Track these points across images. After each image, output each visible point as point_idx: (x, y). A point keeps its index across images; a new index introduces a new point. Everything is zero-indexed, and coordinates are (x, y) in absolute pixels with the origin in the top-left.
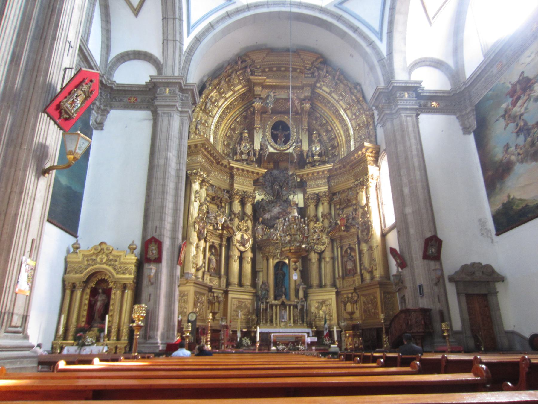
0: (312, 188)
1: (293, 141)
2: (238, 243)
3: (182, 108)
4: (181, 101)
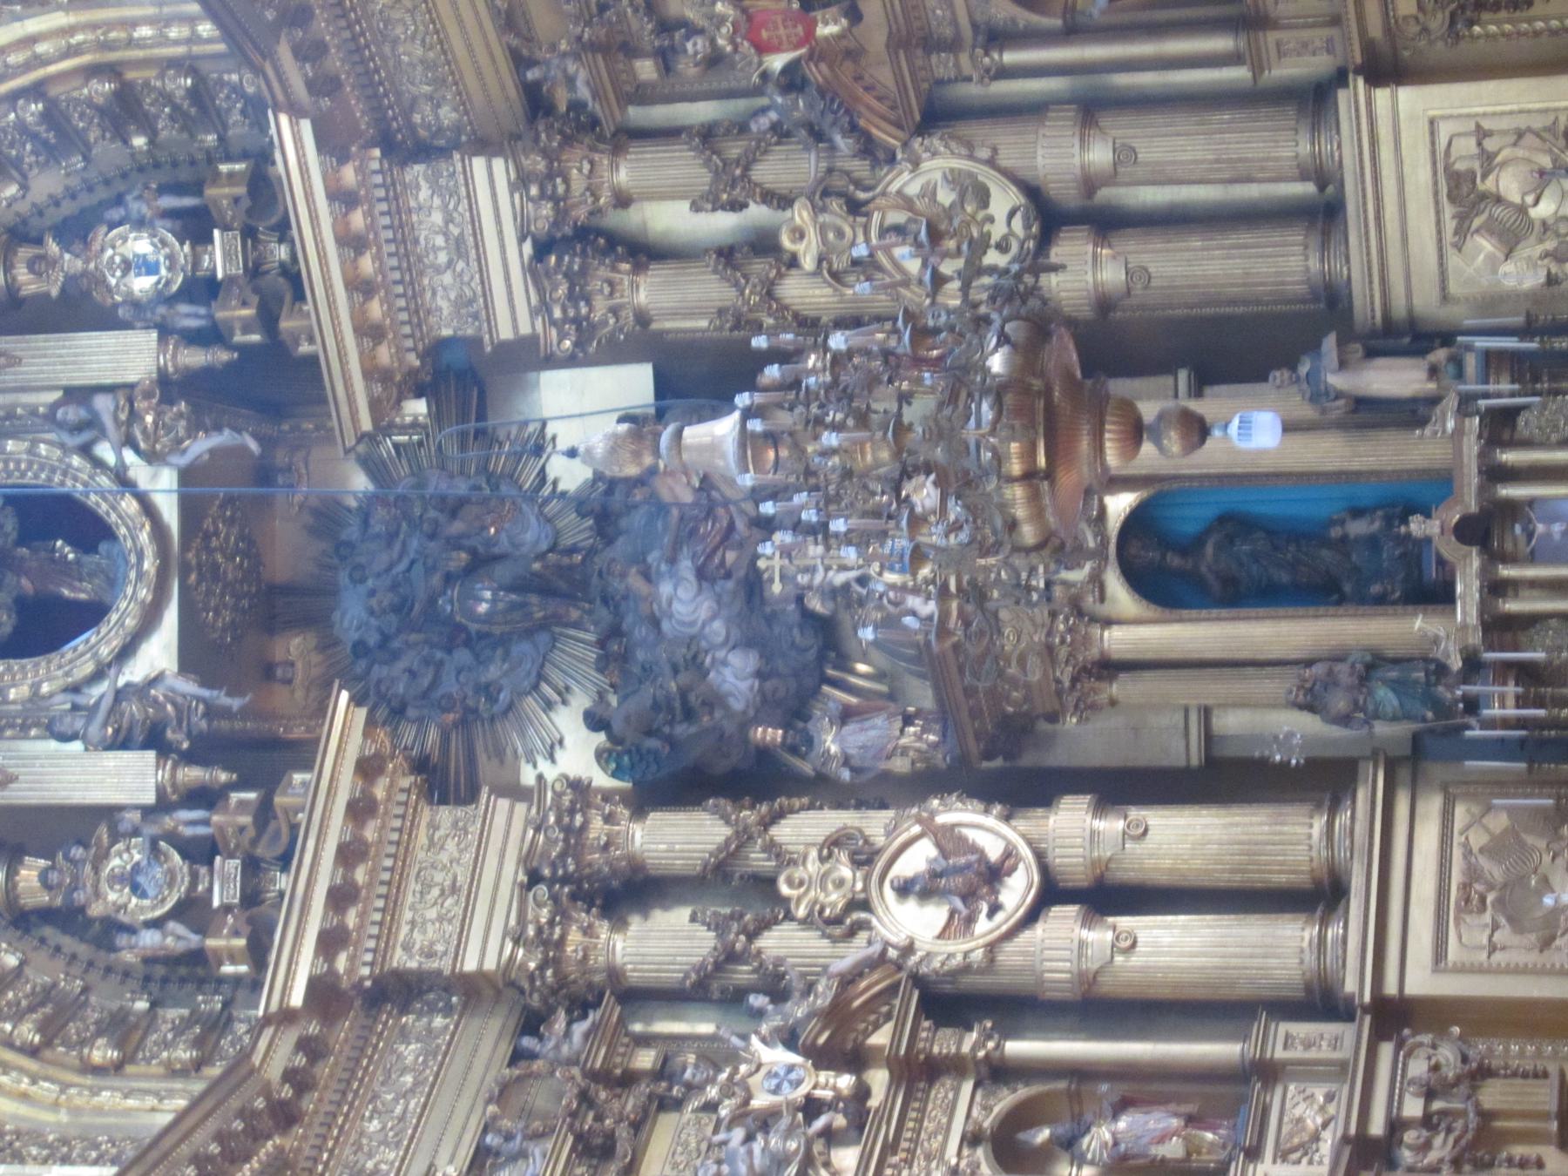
0: (487, 292)
1: (76, 461)
2: (970, 920)
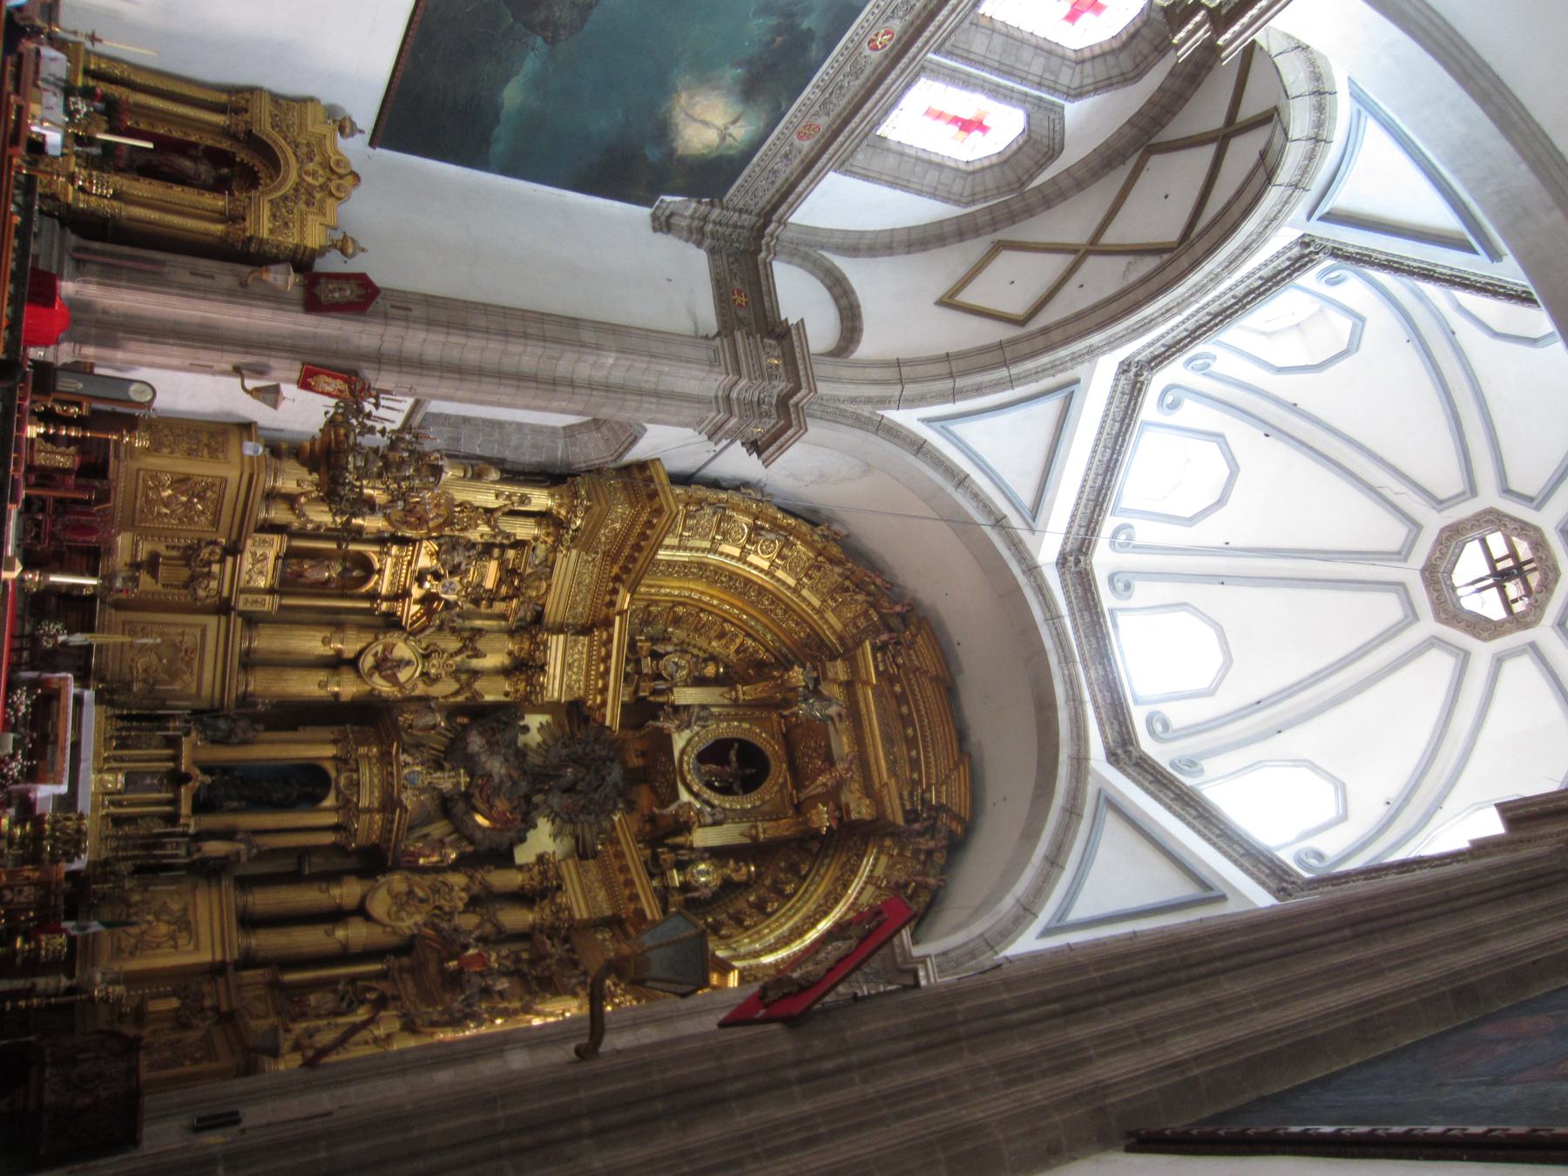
0: (579, 875)
1: (716, 802)
2: (384, 650)
3: (738, 399)
4: (756, 399)
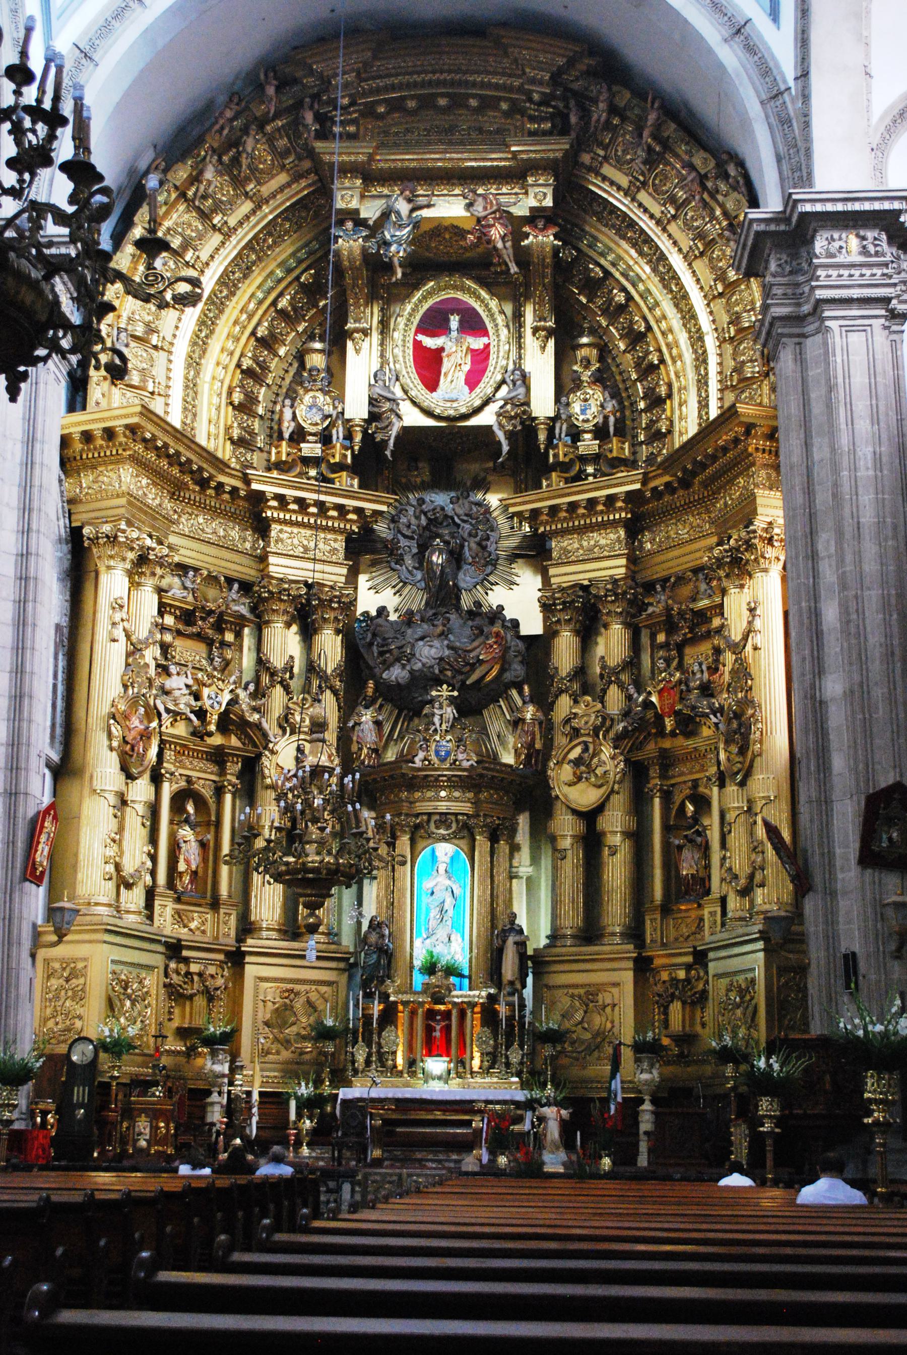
1: (499, 377)
